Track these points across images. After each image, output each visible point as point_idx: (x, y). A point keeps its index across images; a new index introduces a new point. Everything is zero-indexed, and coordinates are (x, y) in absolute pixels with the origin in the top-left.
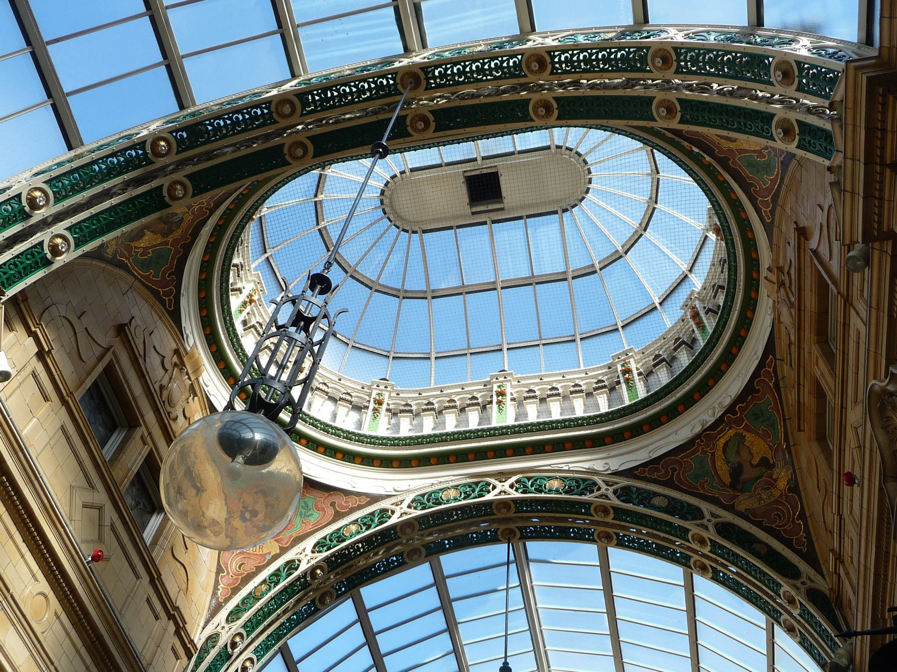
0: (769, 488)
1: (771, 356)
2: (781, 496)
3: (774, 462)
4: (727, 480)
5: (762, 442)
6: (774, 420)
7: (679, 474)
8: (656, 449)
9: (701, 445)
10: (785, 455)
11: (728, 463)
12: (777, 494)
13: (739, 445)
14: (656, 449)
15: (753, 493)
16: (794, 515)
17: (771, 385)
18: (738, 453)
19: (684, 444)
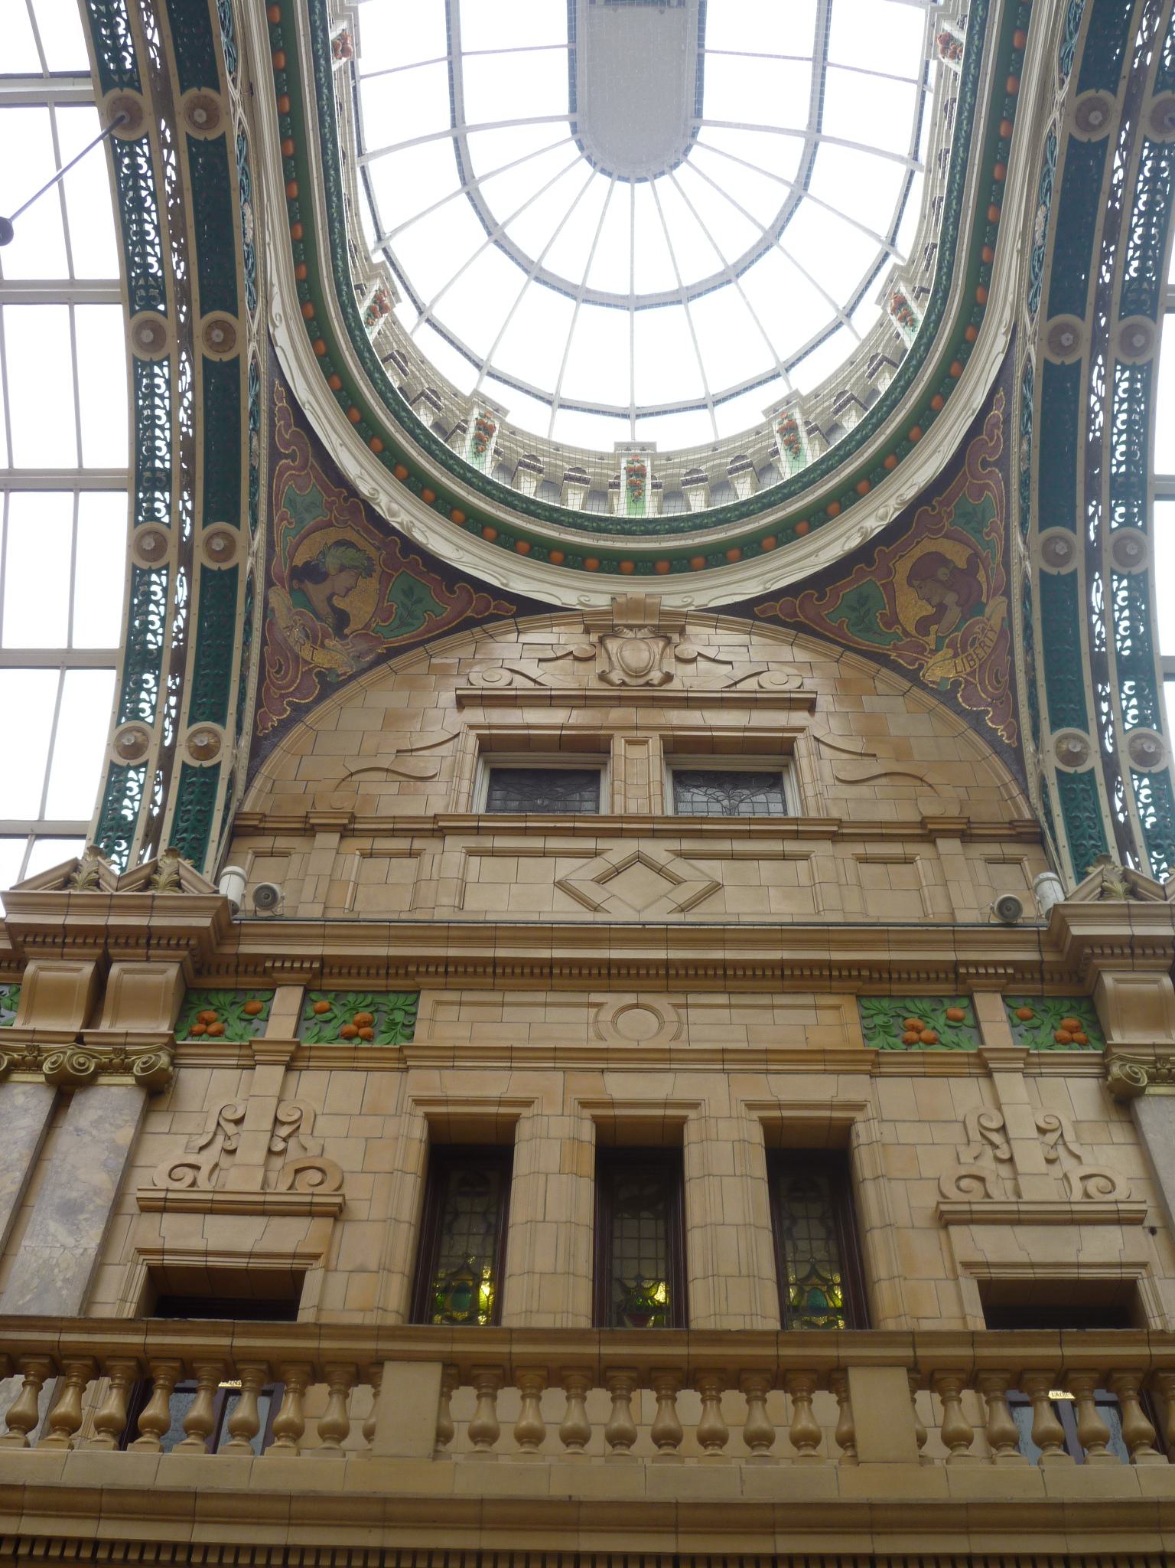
0: (307, 637)
1: (515, 608)
2: (306, 662)
3: (347, 636)
4: (299, 561)
5: (371, 609)
6: (412, 625)
7: (289, 468)
8: (314, 413)
9: (339, 497)
10: (367, 653)
11: (323, 553)
12: (306, 654)
13: (356, 567)
14: (314, 413)
15: (294, 611)
16: (292, 694)
17: (469, 613)
18: (342, 569)
19: (336, 468)
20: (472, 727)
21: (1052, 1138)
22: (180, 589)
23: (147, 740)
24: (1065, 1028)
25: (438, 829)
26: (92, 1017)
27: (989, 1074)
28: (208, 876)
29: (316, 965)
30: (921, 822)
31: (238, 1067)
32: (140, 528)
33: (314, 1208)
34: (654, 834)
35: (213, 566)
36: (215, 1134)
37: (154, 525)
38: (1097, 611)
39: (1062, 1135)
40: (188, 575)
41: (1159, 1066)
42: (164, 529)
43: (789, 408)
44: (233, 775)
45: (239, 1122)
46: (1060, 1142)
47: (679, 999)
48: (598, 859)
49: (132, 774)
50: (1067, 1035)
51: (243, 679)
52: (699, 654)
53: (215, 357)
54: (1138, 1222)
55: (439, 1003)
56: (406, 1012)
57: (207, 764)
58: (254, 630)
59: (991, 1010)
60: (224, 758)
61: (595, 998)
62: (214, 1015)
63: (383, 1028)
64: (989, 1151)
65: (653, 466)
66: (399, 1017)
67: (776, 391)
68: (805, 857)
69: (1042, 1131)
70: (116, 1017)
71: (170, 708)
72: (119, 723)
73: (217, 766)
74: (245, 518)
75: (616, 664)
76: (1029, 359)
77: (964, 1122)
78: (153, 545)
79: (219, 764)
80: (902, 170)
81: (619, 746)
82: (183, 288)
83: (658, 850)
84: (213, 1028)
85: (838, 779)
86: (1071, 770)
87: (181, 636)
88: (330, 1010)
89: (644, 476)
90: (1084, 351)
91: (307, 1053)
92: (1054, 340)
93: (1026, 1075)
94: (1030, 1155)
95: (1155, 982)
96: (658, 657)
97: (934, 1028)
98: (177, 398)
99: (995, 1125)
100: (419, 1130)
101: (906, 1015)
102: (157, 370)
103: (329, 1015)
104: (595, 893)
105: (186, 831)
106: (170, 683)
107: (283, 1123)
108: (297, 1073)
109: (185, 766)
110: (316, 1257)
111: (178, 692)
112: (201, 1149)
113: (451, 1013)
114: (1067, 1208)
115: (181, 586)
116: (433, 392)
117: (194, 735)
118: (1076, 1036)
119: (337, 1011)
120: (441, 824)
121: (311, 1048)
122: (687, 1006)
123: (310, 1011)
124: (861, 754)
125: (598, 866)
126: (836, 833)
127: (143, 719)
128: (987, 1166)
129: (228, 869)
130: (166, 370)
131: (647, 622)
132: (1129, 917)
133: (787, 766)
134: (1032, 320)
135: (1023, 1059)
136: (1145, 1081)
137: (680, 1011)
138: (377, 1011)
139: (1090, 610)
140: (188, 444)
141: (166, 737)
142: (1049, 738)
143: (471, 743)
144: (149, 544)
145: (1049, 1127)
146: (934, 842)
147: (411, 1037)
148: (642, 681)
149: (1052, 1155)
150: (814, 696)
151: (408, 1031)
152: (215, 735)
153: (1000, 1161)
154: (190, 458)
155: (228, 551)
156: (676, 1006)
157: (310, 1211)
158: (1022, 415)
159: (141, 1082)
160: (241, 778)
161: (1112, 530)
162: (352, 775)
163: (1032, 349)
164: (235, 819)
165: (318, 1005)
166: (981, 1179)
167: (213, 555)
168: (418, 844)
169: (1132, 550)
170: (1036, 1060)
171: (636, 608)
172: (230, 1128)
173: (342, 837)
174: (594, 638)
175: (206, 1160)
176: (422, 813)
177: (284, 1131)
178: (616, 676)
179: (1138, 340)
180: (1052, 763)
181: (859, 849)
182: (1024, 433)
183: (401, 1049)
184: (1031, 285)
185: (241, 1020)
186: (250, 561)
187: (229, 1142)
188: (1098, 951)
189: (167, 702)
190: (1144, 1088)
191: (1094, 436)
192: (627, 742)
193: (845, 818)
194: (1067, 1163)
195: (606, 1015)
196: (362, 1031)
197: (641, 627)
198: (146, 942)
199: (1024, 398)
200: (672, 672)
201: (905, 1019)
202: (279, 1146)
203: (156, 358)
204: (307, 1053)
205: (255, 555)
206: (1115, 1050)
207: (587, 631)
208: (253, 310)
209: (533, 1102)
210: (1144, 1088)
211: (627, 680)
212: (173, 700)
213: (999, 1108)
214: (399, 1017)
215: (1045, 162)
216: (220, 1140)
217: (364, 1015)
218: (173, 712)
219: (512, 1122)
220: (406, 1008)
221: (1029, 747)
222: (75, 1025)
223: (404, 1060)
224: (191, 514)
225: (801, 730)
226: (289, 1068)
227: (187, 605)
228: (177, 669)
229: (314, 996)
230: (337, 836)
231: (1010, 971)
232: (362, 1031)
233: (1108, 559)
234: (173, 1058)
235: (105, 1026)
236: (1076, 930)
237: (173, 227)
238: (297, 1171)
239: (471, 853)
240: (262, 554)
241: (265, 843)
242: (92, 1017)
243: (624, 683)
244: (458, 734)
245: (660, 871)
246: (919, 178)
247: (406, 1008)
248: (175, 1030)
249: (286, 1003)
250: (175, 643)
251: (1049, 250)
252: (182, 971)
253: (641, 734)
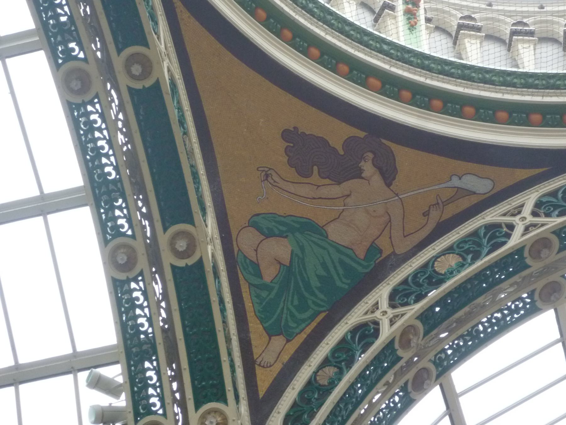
32: (111, 245)
35: (181, 263)
42: (130, 241)
53: (138, 86)
102: (90, 108)
106: (169, 373)
127: (155, 413)
130: (98, 106)
144: (122, 259)
155: (192, 246)
186: (210, 248)
212: (175, 385)
218: (177, 395)
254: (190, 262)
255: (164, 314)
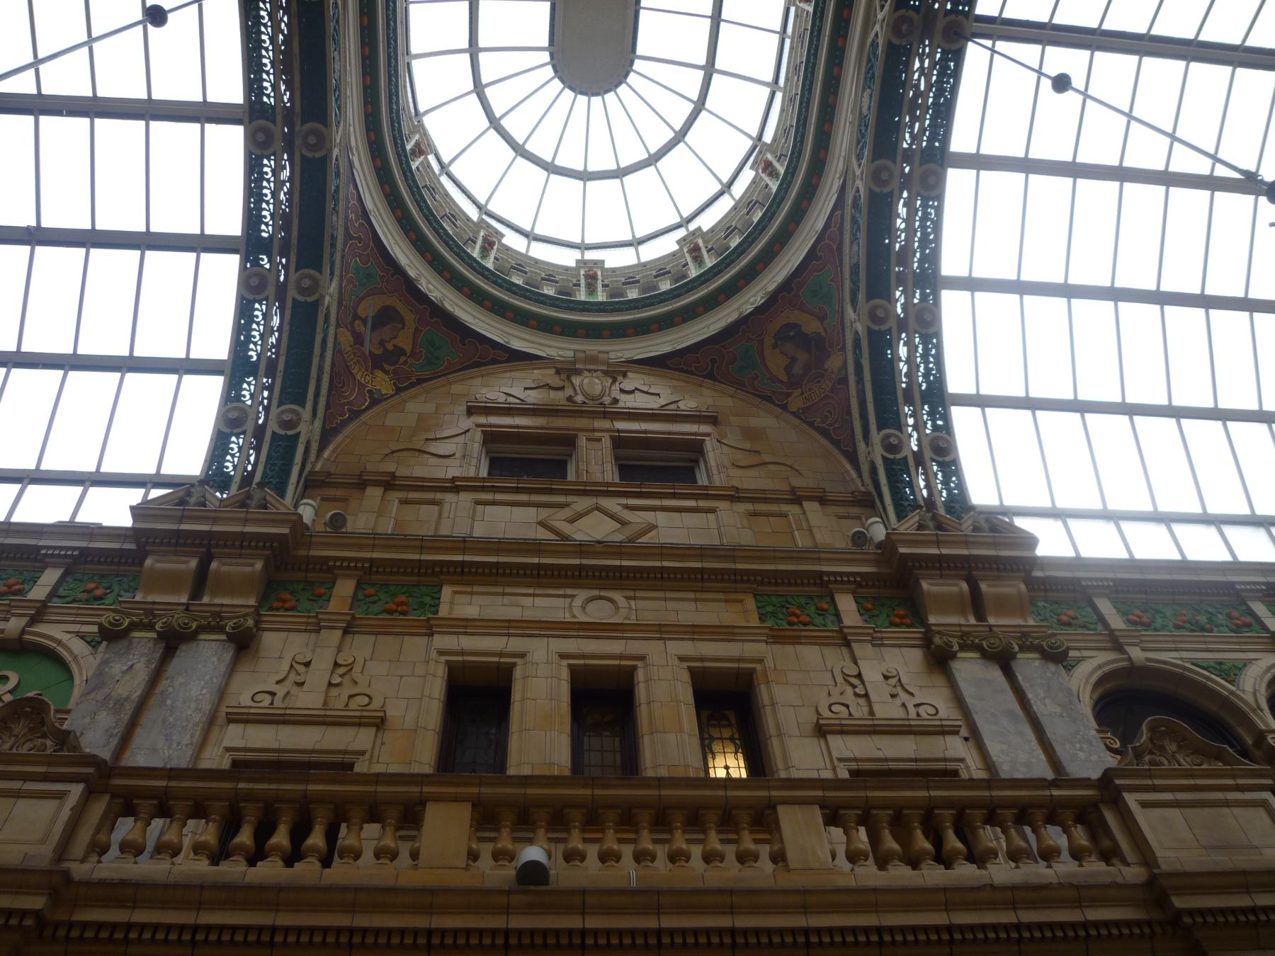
20: (478, 426)
21: (893, 681)
22: (275, 318)
23: (247, 417)
24: (897, 616)
25: (455, 486)
26: (196, 594)
27: (848, 644)
28: (288, 500)
29: (367, 565)
30: (792, 491)
31: (306, 631)
32: (247, 272)
33: (363, 720)
34: (607, 494)
36: (289, 673)
37: (257, 269)
38: (904, 359)
39: (899, 680)
40: (282, 308)
41: (965, 638)
43: (695, 238)
44: (308, 443)
45: (307, 664)
46: (898, 684)
47: (631, 594)
48: (567, 510)
49: (234, 439)
50: (898, 620)
51: (319, 380)
52: (636, 389)
54: (957, 733)
55: (456, 592)
56: (433, 598)
57: (290, 433)
58: (328, 349)
59: (846, 604)
60: (303, 429)
61: (569, 591)
62: (289, 597)
63: (415, 607)
64: (849, 690)
65: (602, 275)
66: (427, 600)
67: (682, 233)
68: (712, 511)
69: (886, 678)
70: (214, 594)
71: (263, 398)
72: (226, 404)
73: (298, 434)
74: (326, 269)
75: (579, 391)
76: (858, 191)
77: (832, 671)
78: (257, 282)
79: (299, 433)
80: (767, 91)
81: (582, 441)
82: (289, 113)
83: (612, 504)
84: (287, 605)
85: (734, 465)
86: (891, 457)
87: (274, 350)
88: (376, 595)
89: (597, 279)
90: (894, 185)
91: (359, 622)
92: (876, 176)
93: (874, 645)
94: (879, 691)
95: (957, 585)
96: (608, 390)
97: (808, 615)
98: (279, 184)
99: (855, 673)
100: (441, 672)
101: (788, 606)
102: (265, 162)
103: (375, 598)
104: (567, 529)
105: (272, 477)
107: (341, 666)
108: (351, 635)
109: (274, 433)
110: (363, 753)
111: (270, 388)
112: (278, 682)
113: (465, 598)
114: (907, 723)
115: (276, 315)
116: (452, 215)
117: (283, 412)
118: (904, 621)
119: (381, 595)
120: (457, 483)
121: (361, 618)
122: (635, 598)
123: (360, 596)
124: (749, 451)
125: (567, 513)
126: (735, 496)
127: (244, 402)
128: (849, 697)
129: (304, 501)
130: (272, 162)
131: (600, 368)
132: (938, 543)
133: (697, 461)
134: (860, 165)
135: (871, 634)
136: (956, 648)
137: (630, 601)
138: (411, 596)
139: (900, 360)
140: (286, 218)
141: (260, 418)
142: (876, 437)
143: (479, 436)
145: (890, 675)
146: (801, 504)
147: (437, 612)
148: (598, 402)
149: (894, 691)
150: (716, 414)
151: (434, 609)
152: (298, 414)
153: (856, 695)
154: (286, 227)
156: (628, 598)
157: (359, 723)
158: (852, 229)
159: (231, 638)
160: (314, 447)
161: (915, 304)
162: (393, 452)
163: (859, 183)
164: (308, 475)
165: (366, 592)
166: (847, 706)
167: (302, 291)
168: (439, 496)
169: (927, 317)
170: (879, 635)
171: (591, 359)
172: (301, 669)
173: (385, 490)
174: (564, 376)
175: (280, 691)
176: (442, 476)
177: (341, 670)
178: (579, 398)
179: (932, 180)
180: (878, 453)
181: (749, 507)
182: (854, 238)
183: (428, 620)
184: (859, 142)
185: (309, 599)
187: (299, 677)
188: (917, 564)
189: (262, 393)
190: (956, 652)
191: (901, 247)
192: (587, 439)
193: (740, 487)
194: (904, 697)
195: (578, 602)
196: (399, 609)
197: (596, 371)
198: (241, 544)
199: (853, 218)
200: (618, 398)
201: (788, 608)
202: (336, 680)
203: (266, 153)
204: (359, 622)
205: (331, 296)
206: (933, 628)
207: (558, 372)
208: (337, 126)
209: (526, 655)
210: (956, 652)
211: (586, 401)
212: (266, 394)
213: (856, 663)
214: (427, 600)
215: (869, 60)
216: (292, 677)
217: (402, 598)
218: (266, 402)
219: (510, 669)
220: (434, 595)
221: (861, 446)
222: (184, 599)
223: (431, 627)
224: (286, 267)
225: (708, 435)
226: (346, 632)
227: (280, 329)
228: (270, 372)
229: (364, 586)
230: (382, 489)
231: (859, 579)
232: (399, 609)
233: (912, 324)
234: (257, 623)
235: (206, 600)
236: (902, 550)
237: (284, 65)
238: (351, 697)
239: (478, 503)
240: (336, 296)
241: (332, 492)
242: (196, 594)
243: (584, 403)
244: (468, 431)
245: (612, 516)
246: (779, 96)
247: (434, 595)
248: (259, 603)
249: (345, 588)
250: (269, 354)
251: (872, 118)
252: (266, 567)
253: (597, 434)
254: (309, 299)
255: (274, 341)
